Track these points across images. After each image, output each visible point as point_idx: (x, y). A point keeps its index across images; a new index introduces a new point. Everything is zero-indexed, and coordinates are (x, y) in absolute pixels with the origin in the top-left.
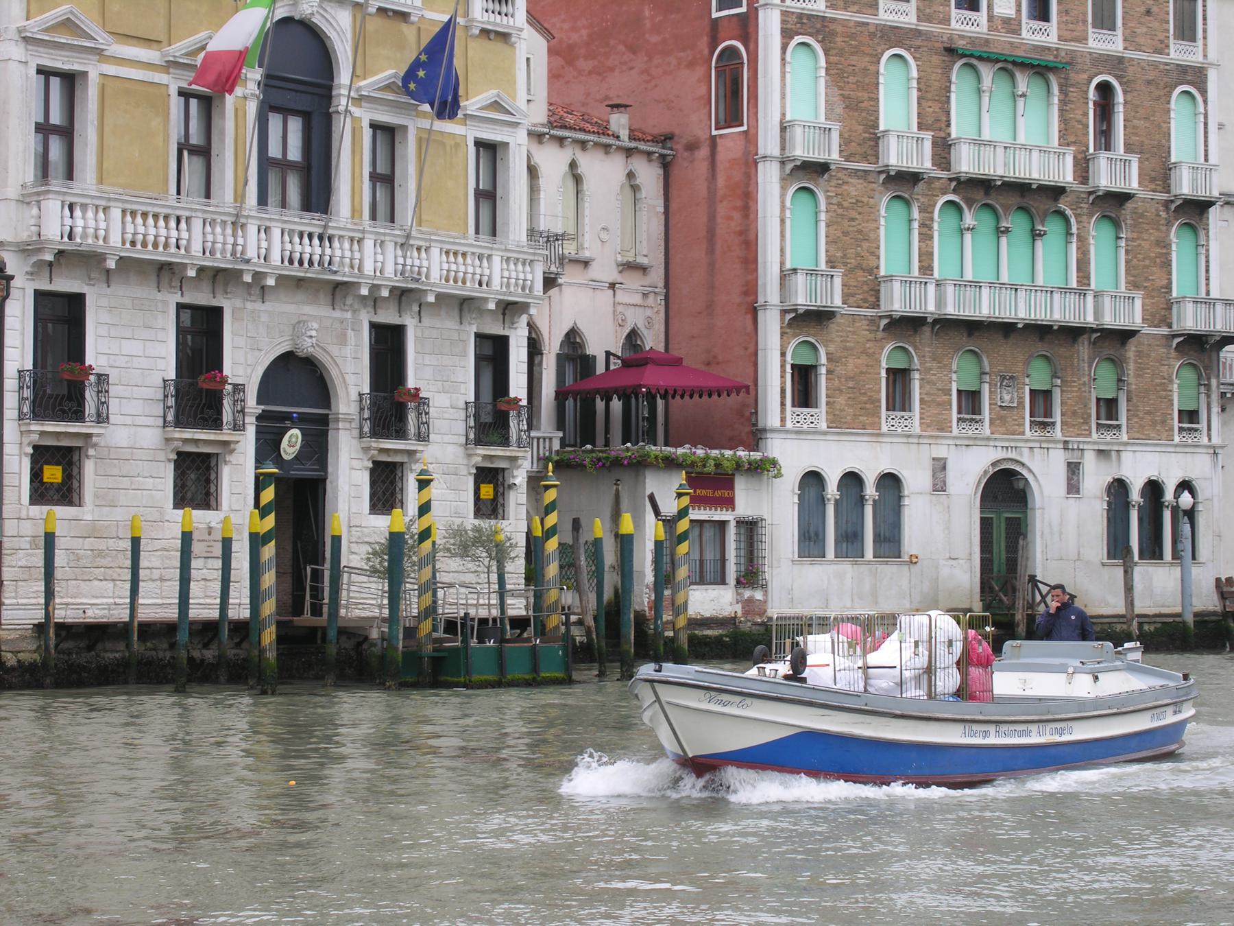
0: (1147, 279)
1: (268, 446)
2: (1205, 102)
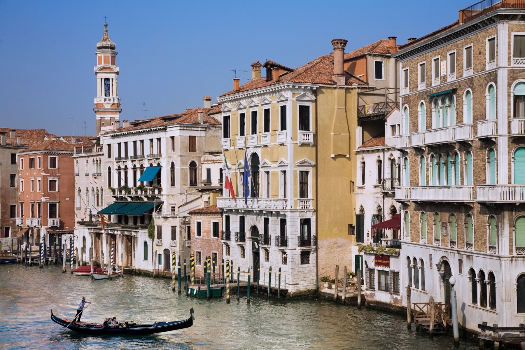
0: (479, 177)
1: (253, 245)
2: (497, 87)
